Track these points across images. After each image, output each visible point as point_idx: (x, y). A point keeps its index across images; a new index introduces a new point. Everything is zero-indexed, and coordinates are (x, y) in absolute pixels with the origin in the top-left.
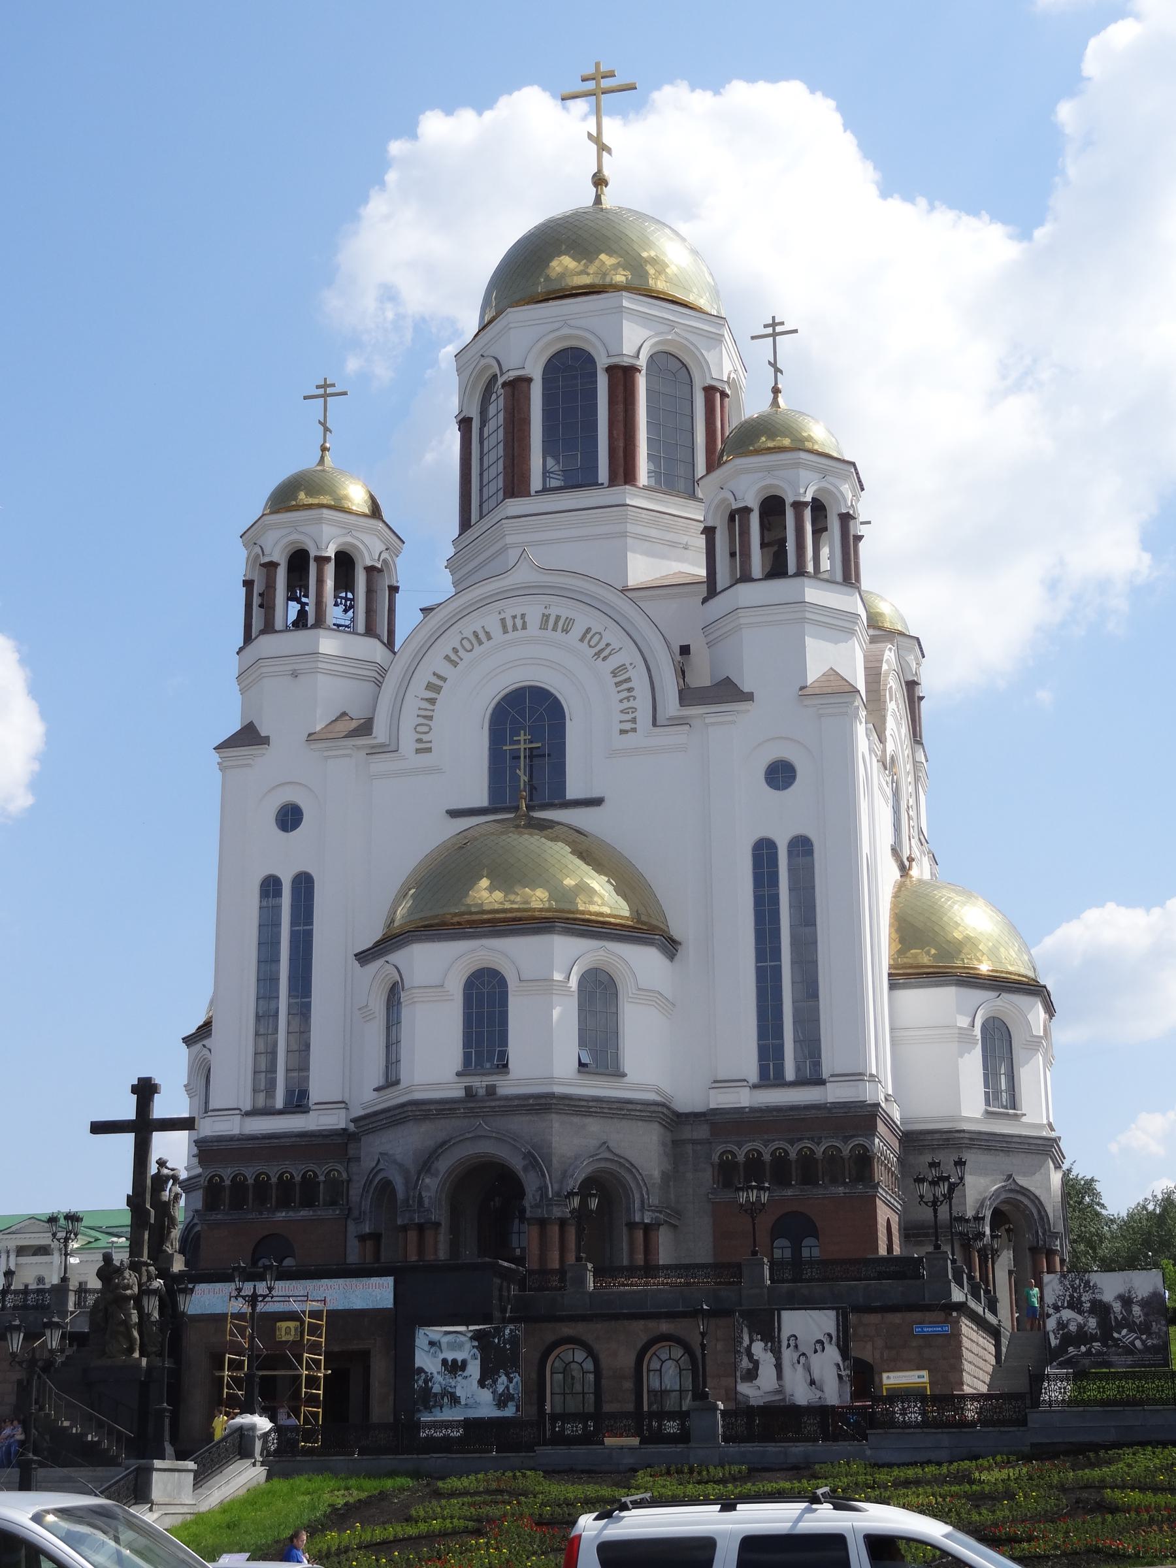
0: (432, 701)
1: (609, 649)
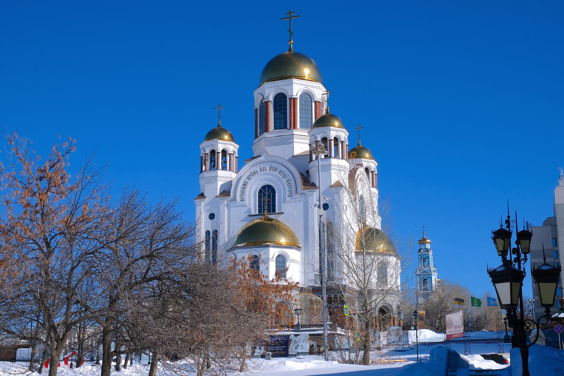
1: (286, 175)
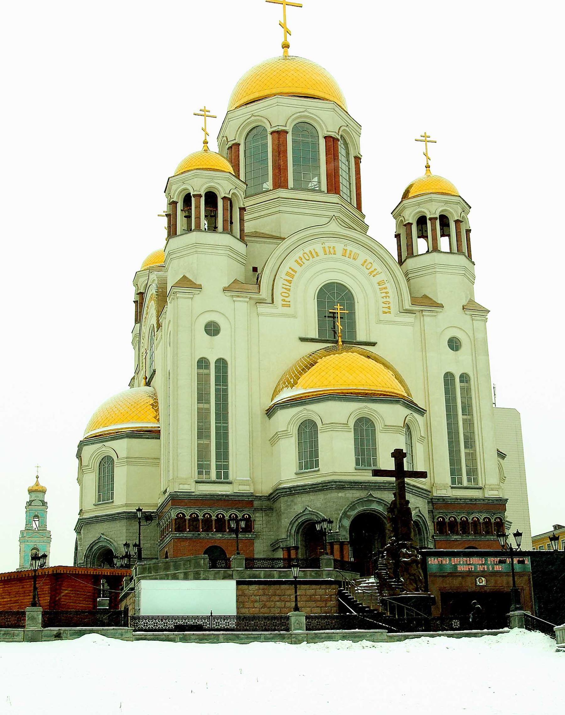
0: (290, 282)
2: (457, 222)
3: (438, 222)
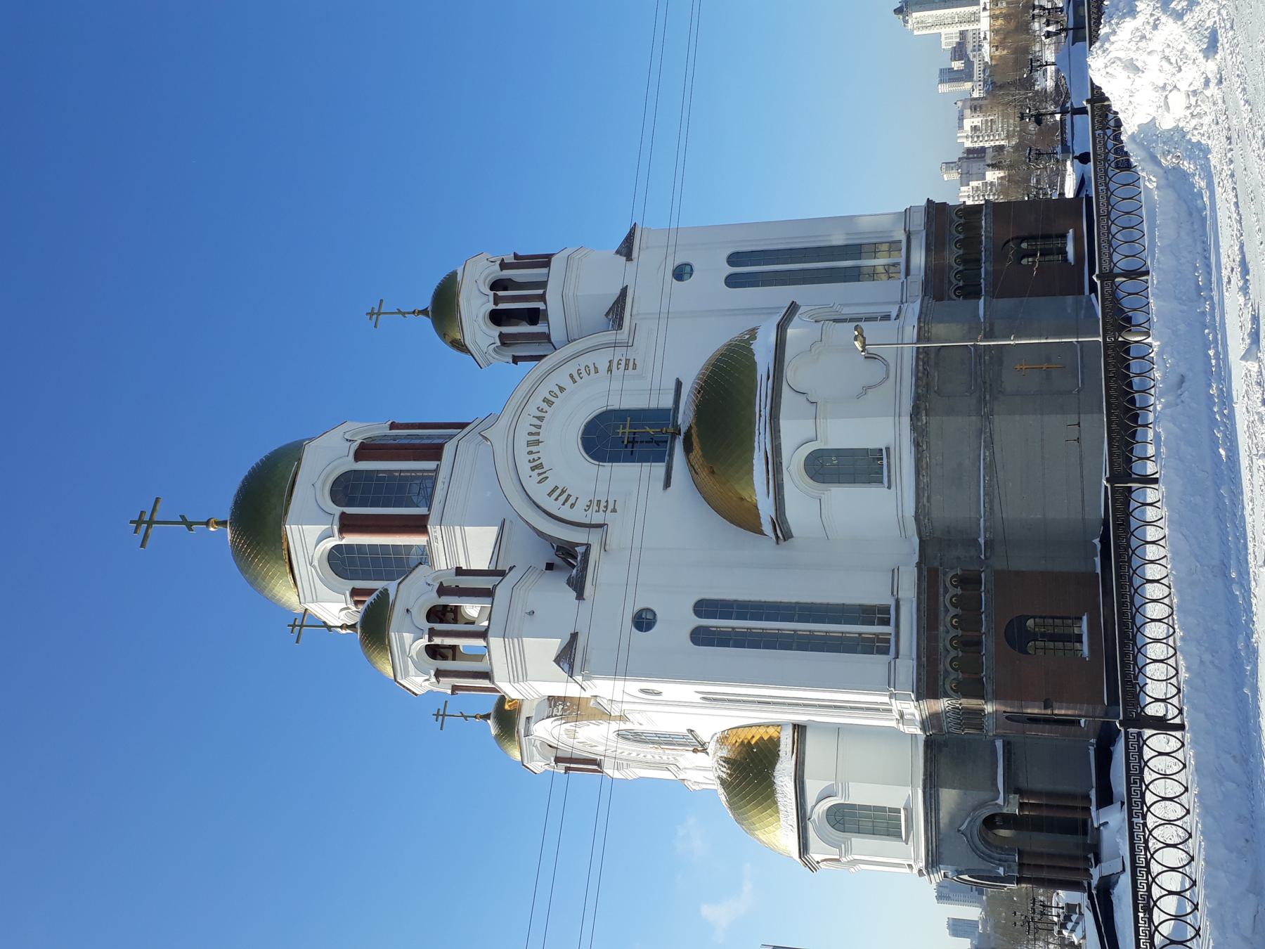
2: (504, 266)
3: (501, 293)
